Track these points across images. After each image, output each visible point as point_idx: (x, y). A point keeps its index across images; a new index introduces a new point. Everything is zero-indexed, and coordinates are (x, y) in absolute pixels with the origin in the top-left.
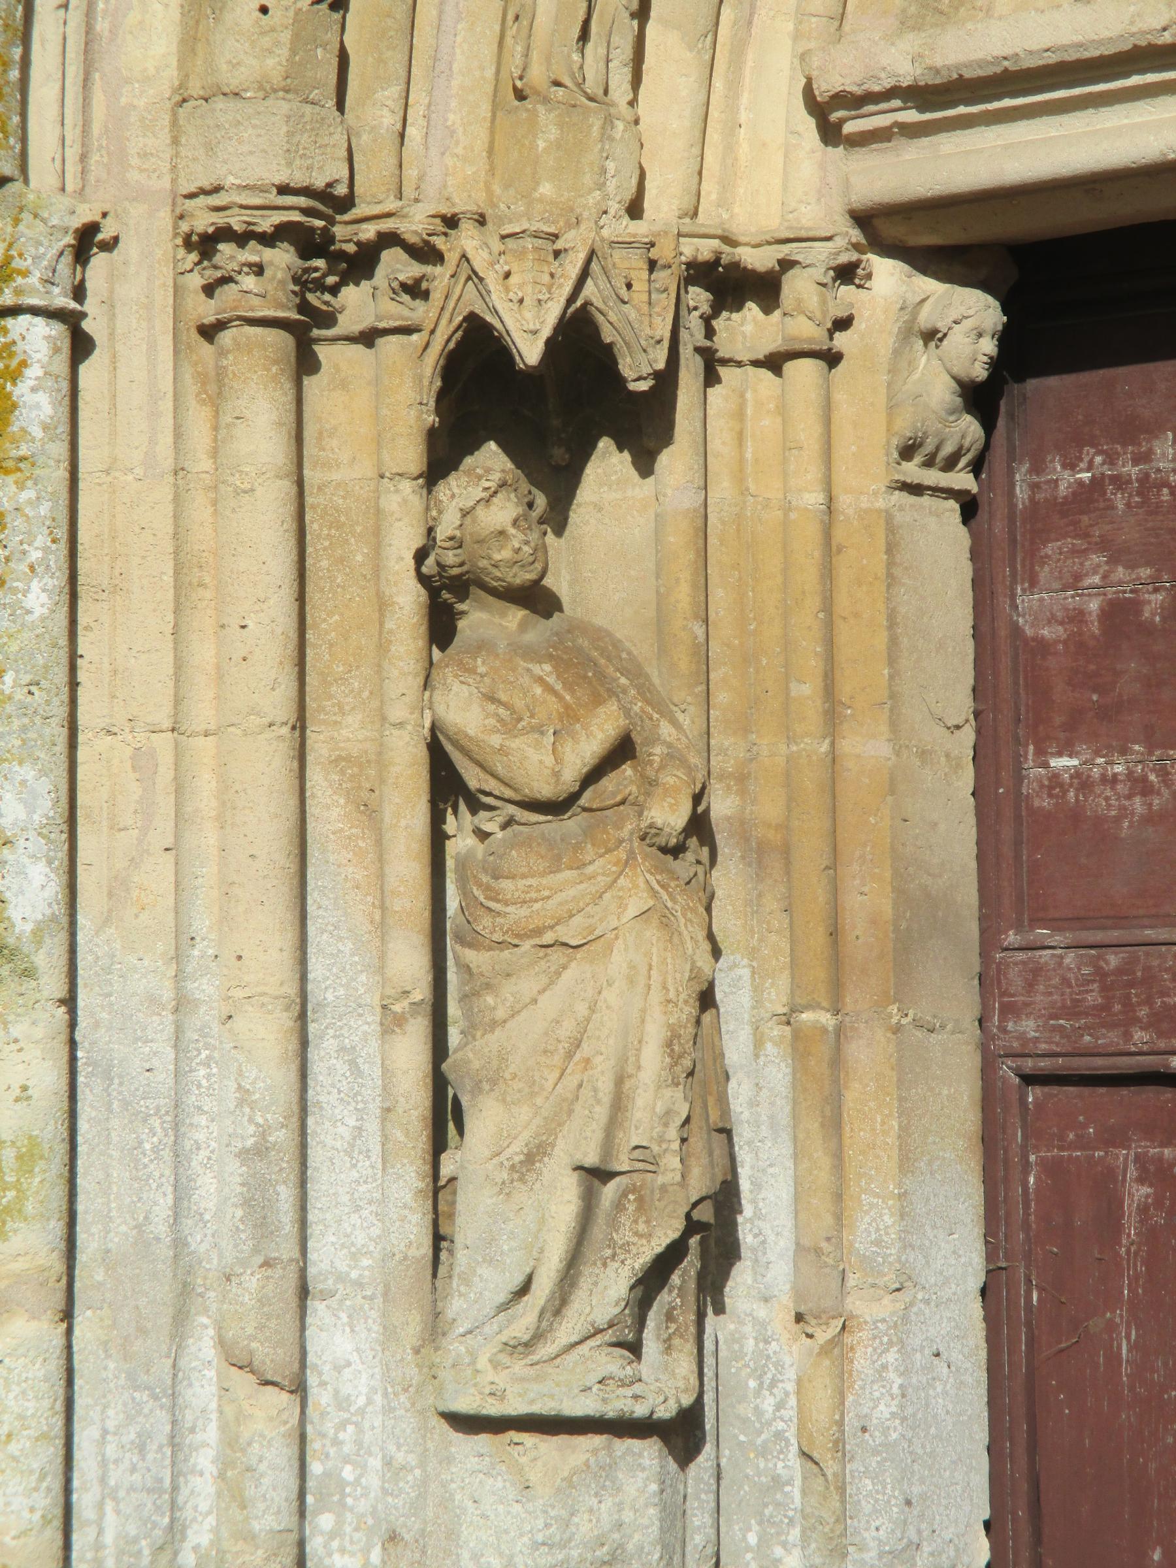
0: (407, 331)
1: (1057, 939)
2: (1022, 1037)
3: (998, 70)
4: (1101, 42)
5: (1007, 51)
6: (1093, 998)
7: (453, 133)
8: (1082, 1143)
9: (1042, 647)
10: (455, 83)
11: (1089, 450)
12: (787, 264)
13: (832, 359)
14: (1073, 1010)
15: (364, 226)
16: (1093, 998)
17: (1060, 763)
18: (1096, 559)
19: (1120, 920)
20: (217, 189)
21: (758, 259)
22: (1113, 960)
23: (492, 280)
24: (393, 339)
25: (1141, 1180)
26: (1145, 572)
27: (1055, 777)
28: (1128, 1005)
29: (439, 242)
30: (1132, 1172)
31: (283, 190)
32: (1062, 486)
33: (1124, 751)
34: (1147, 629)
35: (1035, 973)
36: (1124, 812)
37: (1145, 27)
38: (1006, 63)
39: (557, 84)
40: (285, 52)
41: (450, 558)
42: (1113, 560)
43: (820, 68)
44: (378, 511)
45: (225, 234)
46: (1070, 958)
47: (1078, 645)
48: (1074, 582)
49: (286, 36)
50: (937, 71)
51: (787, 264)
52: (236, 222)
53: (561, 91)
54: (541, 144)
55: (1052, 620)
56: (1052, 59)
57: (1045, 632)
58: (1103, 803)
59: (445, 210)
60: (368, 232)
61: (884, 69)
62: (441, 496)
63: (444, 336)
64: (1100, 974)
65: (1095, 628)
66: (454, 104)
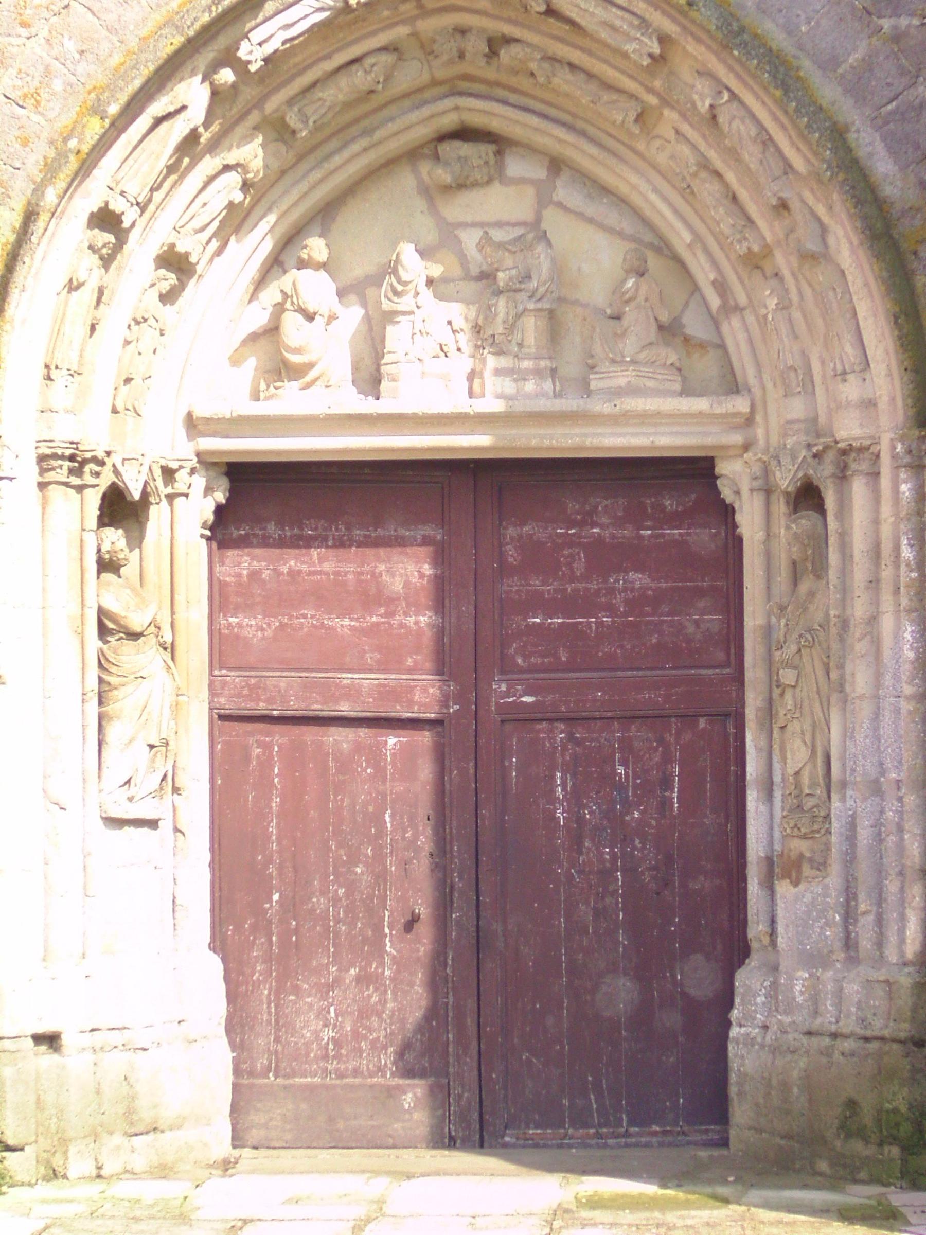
1: (232, 673)
2: (219, 703)
6: (246, 692)
8: (237, 736)
9: (227, 584)
11: (243, 525)
13: (187, 495)
14: (239, 695)
16: (246, 692)
17: (231, 620)
18: (246, 558)
19: (252, 669)
20: (51, 441)
21: (174, 465)
22: (253, 681)
25: (257, 747)
26: (264, 564)
27: (230, 624)
28: (257, 694)
29: (106, 459)
30: (255, 745)
31: (72, 443)
32: (234, 535)
33: (255, 618)
34: (264, 582)
35: (224, 684)
36: (254, 635)
39: (127, 409)
41: (107, 556)
42: (252, 559)
44: (82, 540)
45: (55, 456)
46: (237, 680)
47: (239, 584)
48: (239, 564)
51: (181, 467)
52: (59, 452)
55: (230, 575)
57: (228, 579)
58: (248, 633)
59: (108, 449)
60: (88, 455)
62: (104, 536)
64: (248, 685)
65: (245, 579)
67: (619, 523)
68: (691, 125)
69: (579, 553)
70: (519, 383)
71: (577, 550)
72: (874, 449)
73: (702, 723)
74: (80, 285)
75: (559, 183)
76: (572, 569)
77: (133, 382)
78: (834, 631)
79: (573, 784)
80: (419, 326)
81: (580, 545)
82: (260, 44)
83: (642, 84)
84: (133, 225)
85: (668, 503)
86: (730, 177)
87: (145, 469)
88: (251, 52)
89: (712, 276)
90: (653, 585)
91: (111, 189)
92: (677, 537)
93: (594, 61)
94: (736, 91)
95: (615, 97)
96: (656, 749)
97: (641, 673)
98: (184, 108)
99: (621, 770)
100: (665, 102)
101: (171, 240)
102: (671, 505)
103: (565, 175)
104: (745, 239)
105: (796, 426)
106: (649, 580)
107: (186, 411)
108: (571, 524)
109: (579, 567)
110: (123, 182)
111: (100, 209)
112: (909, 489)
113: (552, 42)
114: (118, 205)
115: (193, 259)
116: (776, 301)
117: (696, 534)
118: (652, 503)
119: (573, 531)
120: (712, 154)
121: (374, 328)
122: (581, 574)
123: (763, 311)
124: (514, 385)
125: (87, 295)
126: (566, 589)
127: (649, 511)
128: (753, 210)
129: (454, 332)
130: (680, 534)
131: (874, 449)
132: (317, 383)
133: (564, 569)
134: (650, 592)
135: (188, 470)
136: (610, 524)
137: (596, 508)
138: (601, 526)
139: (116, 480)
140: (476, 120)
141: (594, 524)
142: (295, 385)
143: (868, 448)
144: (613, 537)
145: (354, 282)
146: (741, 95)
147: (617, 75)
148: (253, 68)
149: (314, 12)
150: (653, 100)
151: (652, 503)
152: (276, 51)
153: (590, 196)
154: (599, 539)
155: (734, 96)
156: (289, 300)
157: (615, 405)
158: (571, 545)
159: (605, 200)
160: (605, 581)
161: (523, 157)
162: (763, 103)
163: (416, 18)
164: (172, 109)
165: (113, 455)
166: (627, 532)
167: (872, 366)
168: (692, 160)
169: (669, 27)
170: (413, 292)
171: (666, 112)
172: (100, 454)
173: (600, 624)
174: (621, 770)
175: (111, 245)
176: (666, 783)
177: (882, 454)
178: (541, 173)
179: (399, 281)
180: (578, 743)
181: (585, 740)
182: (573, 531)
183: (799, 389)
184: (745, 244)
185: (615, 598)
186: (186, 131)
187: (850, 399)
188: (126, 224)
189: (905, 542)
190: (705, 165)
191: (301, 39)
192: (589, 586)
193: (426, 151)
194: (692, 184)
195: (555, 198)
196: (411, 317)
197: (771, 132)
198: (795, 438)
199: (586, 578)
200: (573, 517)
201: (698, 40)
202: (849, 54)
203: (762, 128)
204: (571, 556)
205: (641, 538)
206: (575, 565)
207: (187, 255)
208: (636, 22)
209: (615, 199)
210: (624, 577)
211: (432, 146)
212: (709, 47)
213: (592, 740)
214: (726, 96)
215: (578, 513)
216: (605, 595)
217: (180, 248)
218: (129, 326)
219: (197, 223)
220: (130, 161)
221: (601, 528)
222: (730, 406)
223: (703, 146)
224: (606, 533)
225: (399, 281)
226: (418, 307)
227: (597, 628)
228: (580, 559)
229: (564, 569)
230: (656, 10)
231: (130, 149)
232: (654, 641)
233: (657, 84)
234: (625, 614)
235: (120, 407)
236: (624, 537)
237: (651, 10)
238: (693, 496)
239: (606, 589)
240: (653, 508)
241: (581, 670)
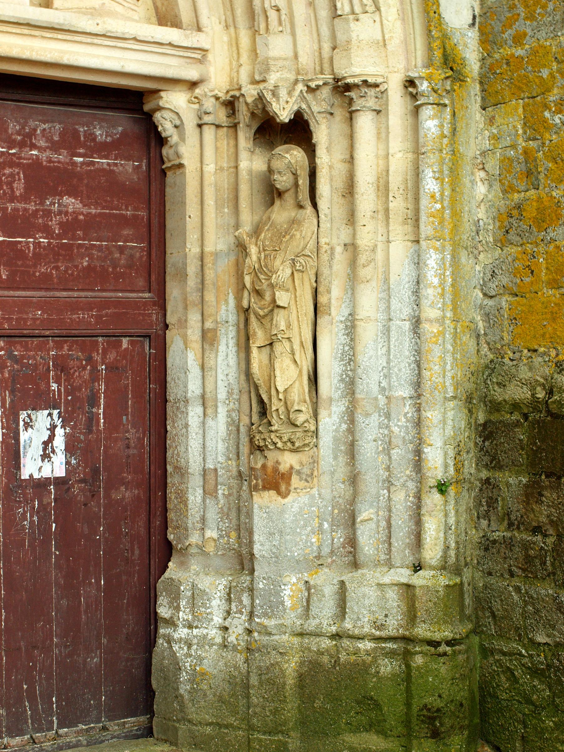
67: (55, 147)
69: (18, 174)
71: (17, 170)
72: (382, 88)
73: (125, 342)
76: (12, 189)
78: (325, 257)
79: (12, 401)
81: (19, 165)
85: (98, 133)
90: (85, 210)
92: (105, 166)
96: (84, 368)
97: (76, 294)
99: (54, 386)
102: (101, 135)
105: (280, 63)
106: (80, 205)
108: (11, 144)
109: (19, 187)
112: (435, 126)
117: (121, 165)
118: (85, 131)
119: (13, 151)
122: (21, 194)
126: (7, 208)
127: (82, 139)
130: (108, 164)
131: (382, 88)
133: (5, 187)
134: (81, 217)
136: (47, 147)
137: (35, 130)
138: (39, 149)
141: (33, 146)
143: (376, 86)
144: (50, 161)
151: (85, 131)
154: (37, 162)
158: (12, 164)
160: (42, 203)
166: (62, 157)
167: (382, 9)
173: (37, 245)
174: (54, 386)
176: (93, 401)
177: (390, 93)
180: (16, 360)
181: (23, 357)
182: (13, 151)
185: (51, 220)
187: (361, 38)
189: (431, 174)
192: (28, 206)
198: (278, 74)
199: (25, 198)
200: (14, 137)
204: (12, 175)
205: (74, 164)
206: (15, 185)
210: (59, 200)
213: (29, 358)
215: (18, 133)
216: (42, 217)
221: (39, 151)
222: (195, 40)
224: (44, 156)
227: (35, 248)
228: (19, 179)
229: (5, 187)
232: (85, 264)
234: (60, 237)
236: (59, 162)
238: (120, 129)
239: (43, 211)
240: (85, 136)
241: (18, 289)
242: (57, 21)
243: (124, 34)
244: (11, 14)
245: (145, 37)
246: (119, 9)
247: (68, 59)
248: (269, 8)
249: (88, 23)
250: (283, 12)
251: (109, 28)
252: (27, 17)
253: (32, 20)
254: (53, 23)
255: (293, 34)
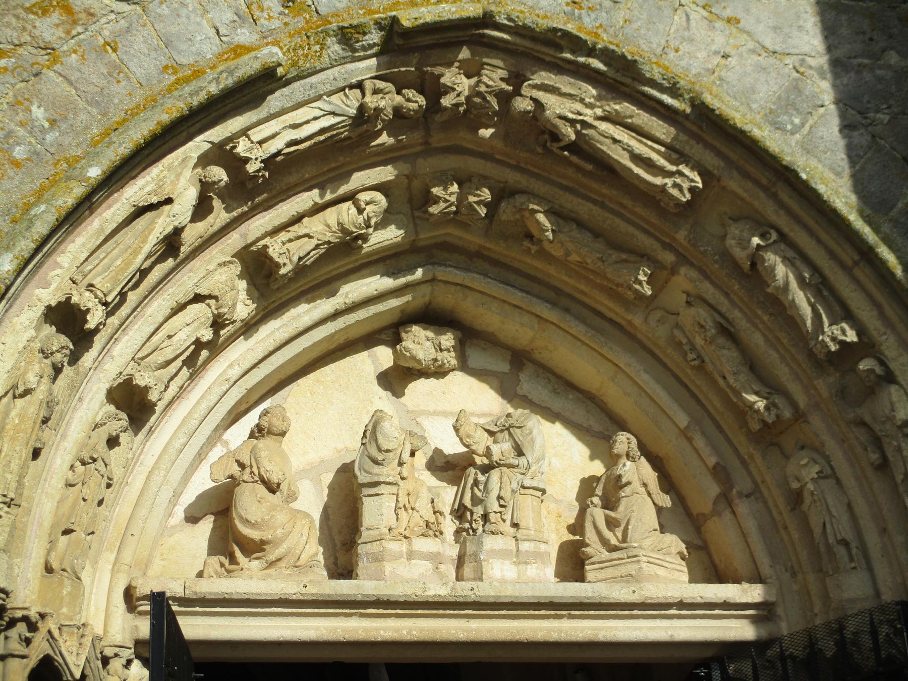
0: (23, 657)
3: (222, 597)
4: (268, 594)
5: (228, 591)
7: (29, 581)
10: (32, 561)
12: (116, 655)
15: (18, 611)
21: (109, 652)
23: (61, 642)
24: (17, 660)
29: (40, 625)
37: (287, 592)
38: (226, 595)
39: (64, 570)
40: (6, 535)
43: (142, 584)
49: (7, 529)
50: (196, 593)
51: (116, 655)
53: (66, 574)
54: (65, 592)
56: (246, 597)
59: (42, 611)
60: (19, 614)
61: (169, 589)
63: (32, 662)
66: (31, 570)
68: (712, 283)
70: (521, 566)
74: (27, 392)
75: (523, 377)
77: (73, 534)
80: (403, 500)
82: (261, 143)
83: (657, 239)
84: (96, 331)
86: (756, 340)
87: (87, 641)
88: (250, 150)
89: (712, 461)
91: (74, 282)
93: (607, 215)
94: (786, 230)
95: (624, 256)
98: (169, 201)
100: (683, 259)
101: (128, 371)
103: (529, 369)
104: (775, 405)
107: (124, 587)
110: (89, 276)
111: (60, 303)
113: (561, 192)
114: (83, 299)
115: (153, 396)
116: (817, 468)
120: (736, 315)
121: (331, 517)
123: (795, 485)
124: (514, 568)
125: (30, 407)
128: (783, 373)
129: (435, 513)
132: (280, 564)
135: (124, 662)
139: (52, 653)
140: (447, 299)
142: (255, 564)
145: (308, 467)
146: (791, 234)
147: (631, 229)
148: (251, 168)
149: (324, 115)
150: (669, 258)
152: (279, 153)
153: (554, 391)
155: (783, 237)
156: (248, 470)
157: (634, 592)
159: (571, 396)
161: (484, 349)
162: (819, 241)
163: (417, 155)
164: (155, 200)
165: (49, 618)
168: (709, 324)
169: (710, 160)
170: (397, 461)
171: (683, 270)
172: (33, 614)
175: (68, 352)
178: (505, 367)
179: (379, 449)
183: (853, 565)
184: (774, 412)
186: (169, 229)
188: (91, 324)
190: (727, 332)
191: (307, 144)
193: (383, 337)
194: (703, 354)
195: (520, 392)
196: (394, 489)
197: (827, 272)
201: (746, 175)
202: (898, 200)
203: (815, 269)
207: (147, 389)
208: (675, 156)
209: (581, 396)
211: (390, 332)
212: (756, 182)
214: (774, 236)
217: (142, 379)
218: (72, 467)
219: (159, 358)
220: (101, 254)
223: (724, 305)
225: (379, 449)
226: (403, 478)
230: (698, 143)
231: (102, 238)
233: (681, 235)
235: (55, 565)
237: (693, 142)
242: (584, 595)
243: (666, 598)
244: (530, 594)
245: (693, 598)
246: (661, 572)
247: (604, 636)
248: (835, 543)
249: (622, 591)
250: (854, 545)
251: (648, 594)
252: (549, 595)
253: (554, 597)
254: (580, 597)
255: (870, 569)
